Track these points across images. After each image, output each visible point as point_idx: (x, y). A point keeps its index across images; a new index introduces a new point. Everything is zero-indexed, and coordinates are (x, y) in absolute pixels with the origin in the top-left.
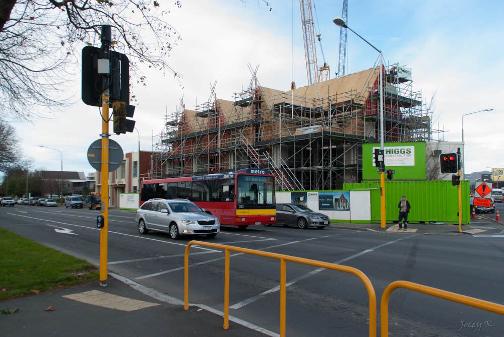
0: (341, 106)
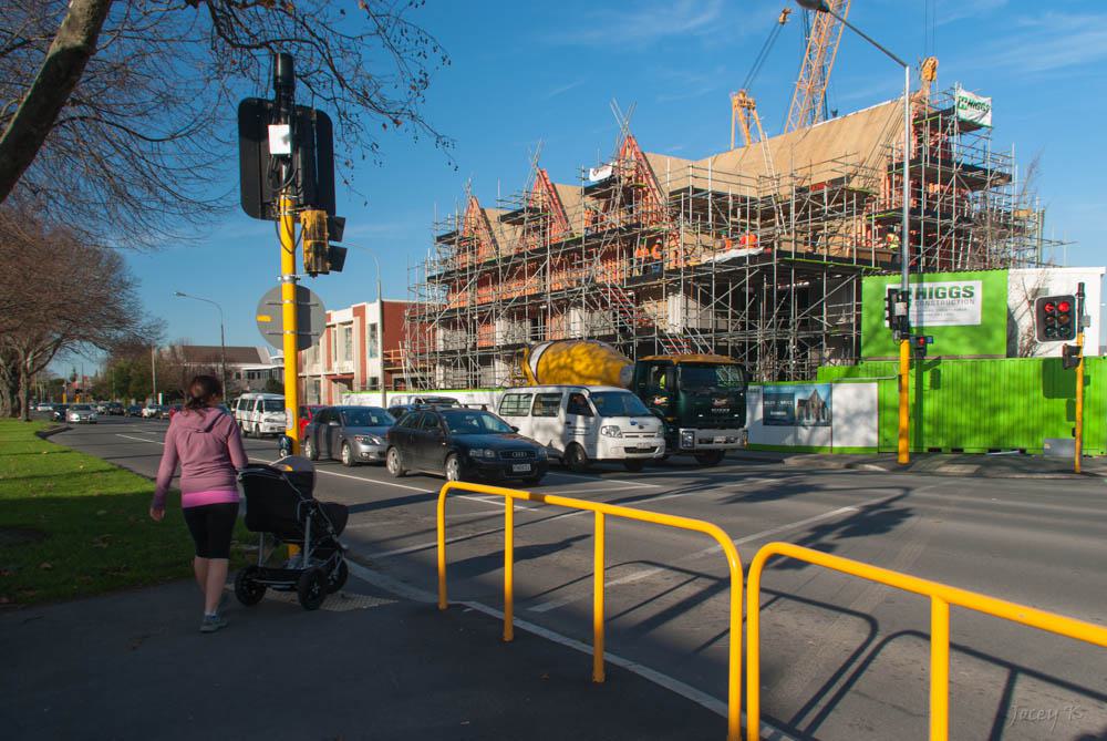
0: (819, 192)
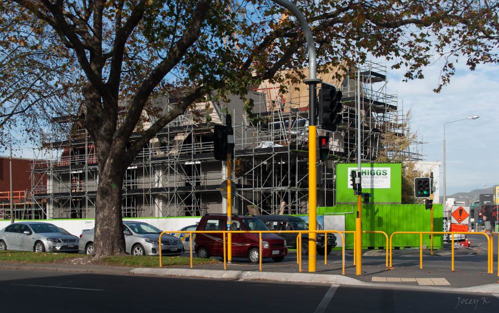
0: (303, 112)
